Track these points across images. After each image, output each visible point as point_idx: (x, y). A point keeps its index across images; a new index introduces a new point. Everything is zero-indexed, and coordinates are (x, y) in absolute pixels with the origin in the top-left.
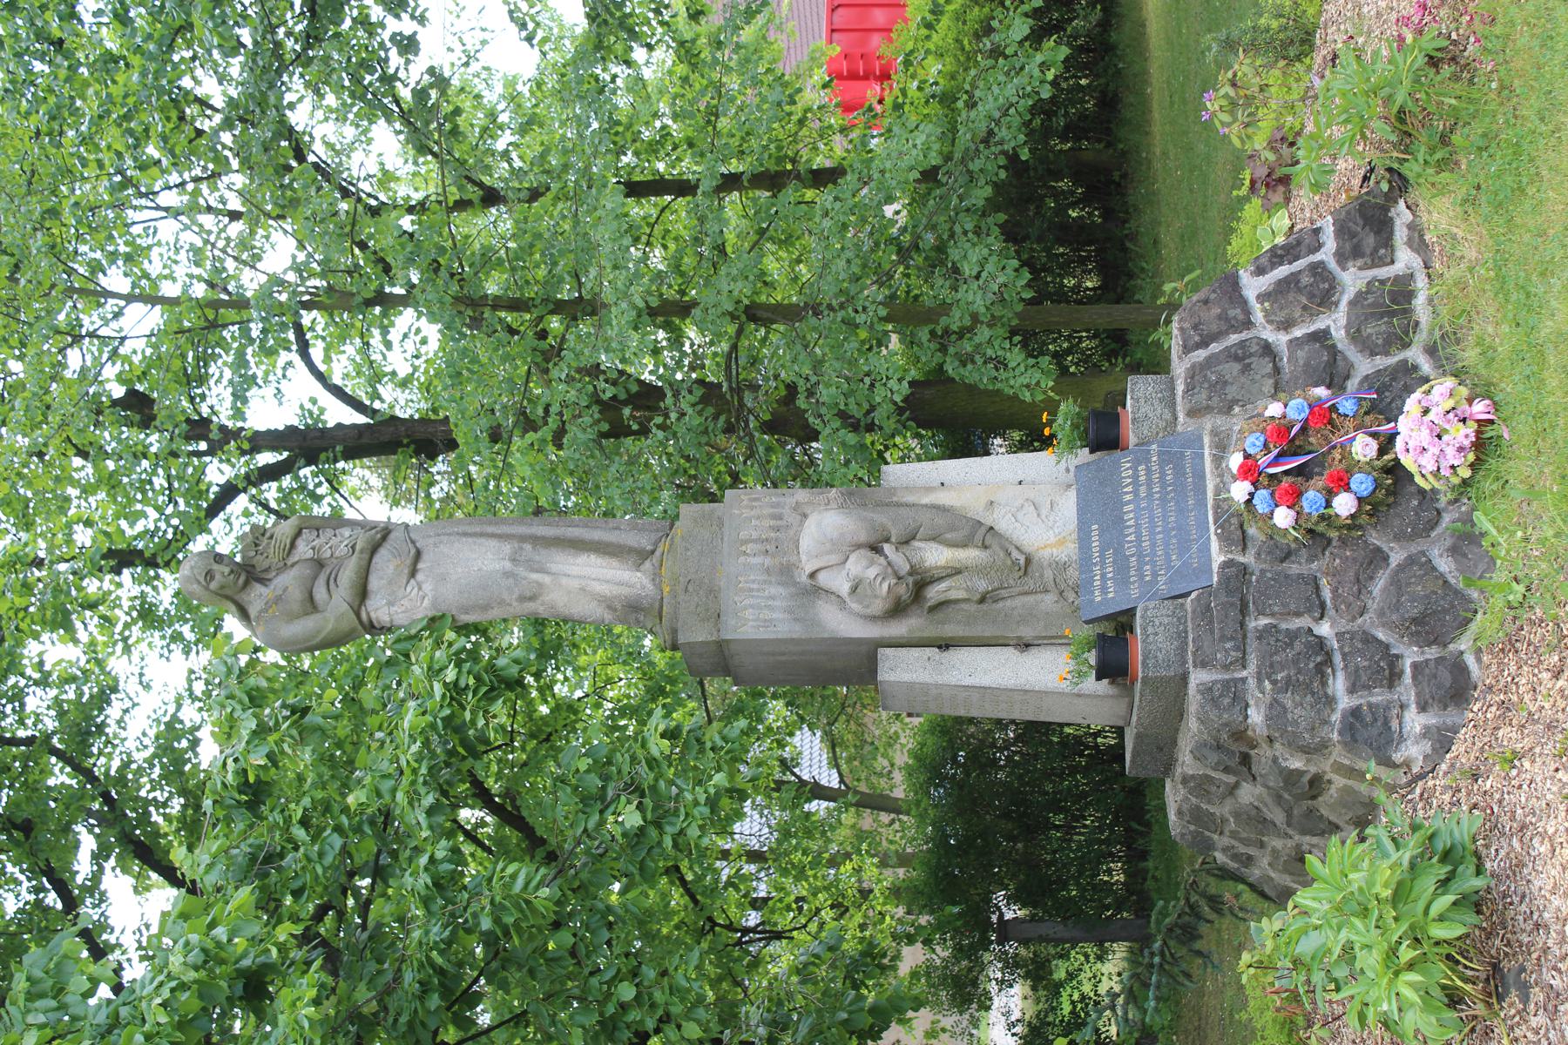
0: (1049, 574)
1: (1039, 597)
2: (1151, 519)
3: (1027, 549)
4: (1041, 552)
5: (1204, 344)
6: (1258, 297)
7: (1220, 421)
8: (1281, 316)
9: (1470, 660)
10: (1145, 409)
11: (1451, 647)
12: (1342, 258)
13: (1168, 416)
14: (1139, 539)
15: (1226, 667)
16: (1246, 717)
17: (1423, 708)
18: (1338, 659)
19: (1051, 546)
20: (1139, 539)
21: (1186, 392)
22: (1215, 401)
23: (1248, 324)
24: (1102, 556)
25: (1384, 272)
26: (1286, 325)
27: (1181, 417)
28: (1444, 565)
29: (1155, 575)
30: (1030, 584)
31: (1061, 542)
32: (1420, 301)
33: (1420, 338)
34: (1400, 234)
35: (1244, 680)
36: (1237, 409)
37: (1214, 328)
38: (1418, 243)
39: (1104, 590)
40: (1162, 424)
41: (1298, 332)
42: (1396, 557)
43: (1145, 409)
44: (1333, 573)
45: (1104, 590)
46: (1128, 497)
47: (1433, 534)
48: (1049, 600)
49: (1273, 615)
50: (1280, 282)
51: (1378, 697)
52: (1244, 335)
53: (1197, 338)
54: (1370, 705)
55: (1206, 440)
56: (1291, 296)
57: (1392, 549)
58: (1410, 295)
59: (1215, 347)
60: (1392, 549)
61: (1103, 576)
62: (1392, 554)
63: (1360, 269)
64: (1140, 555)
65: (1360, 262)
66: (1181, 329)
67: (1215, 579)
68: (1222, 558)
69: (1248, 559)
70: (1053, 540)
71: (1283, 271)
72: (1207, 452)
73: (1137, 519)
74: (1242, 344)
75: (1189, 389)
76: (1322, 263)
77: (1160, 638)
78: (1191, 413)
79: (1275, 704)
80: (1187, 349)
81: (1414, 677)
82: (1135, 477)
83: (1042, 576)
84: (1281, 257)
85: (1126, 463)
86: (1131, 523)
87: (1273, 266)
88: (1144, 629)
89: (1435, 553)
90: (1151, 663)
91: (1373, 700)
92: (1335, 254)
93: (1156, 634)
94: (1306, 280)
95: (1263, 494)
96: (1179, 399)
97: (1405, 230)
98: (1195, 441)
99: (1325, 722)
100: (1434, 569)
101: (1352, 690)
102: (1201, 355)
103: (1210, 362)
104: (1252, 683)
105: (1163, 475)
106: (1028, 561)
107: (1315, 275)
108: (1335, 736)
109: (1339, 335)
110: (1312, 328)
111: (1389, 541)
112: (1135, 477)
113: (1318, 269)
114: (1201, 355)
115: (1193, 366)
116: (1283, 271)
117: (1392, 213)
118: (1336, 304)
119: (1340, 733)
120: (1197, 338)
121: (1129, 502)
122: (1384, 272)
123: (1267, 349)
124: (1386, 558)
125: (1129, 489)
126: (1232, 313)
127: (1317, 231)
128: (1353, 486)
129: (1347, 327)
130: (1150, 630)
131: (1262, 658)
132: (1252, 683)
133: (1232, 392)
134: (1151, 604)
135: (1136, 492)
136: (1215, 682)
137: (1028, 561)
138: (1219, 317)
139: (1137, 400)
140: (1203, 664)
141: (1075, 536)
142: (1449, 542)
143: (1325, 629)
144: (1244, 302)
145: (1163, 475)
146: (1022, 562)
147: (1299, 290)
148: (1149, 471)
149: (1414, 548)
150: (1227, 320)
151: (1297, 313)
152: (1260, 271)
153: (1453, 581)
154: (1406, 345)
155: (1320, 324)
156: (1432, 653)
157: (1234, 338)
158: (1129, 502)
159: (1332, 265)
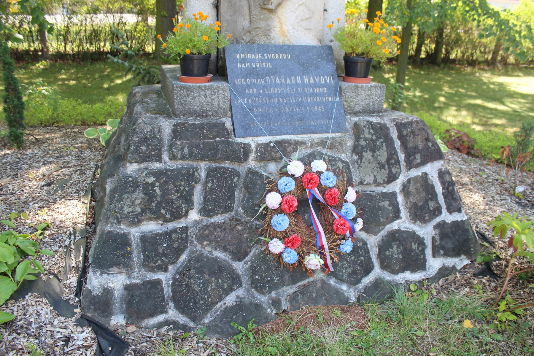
0: (262, 24)
1: (247, 17)
2: (288, 95)
3: (280, 11)
4: (277, 20)
5: (400, 137)
6: (426, 174)
7: (350, 143)
8: (412, 188)
9: (161, 318)
10: (363, 94)
11: (172, 304)
12: (441, 226)
13: (357, 108)
14: (276, 86)
15: (171, 146)
16: (131, 163)
17: (127, 288)
18: (171, 226)
19: (281, 27)
20: (276, 86)
21: (371, 123)
22: (363, 143)
23: (410, 166)
24: (269, 60)
25: (429, 252)
26: (405, 189)
27: (355, 119)
28: (230, 300)
29: (250, 96)
30: (256, 11)
31: (283, 34)
32: (408, 276)
33: (387, 276)
34: (450, 262)
35: (159, 159)
36: (355, 157)
37: (410, 145)
38: (444, 272)
39: (243, 61)
40: (353, 105)
41: (400, 199)
42: (240, 267)
43: (363, 94)
44: (235, 221)
45: (243, 61)
46: (306, 80)
47: (254, 290)
48: (246, 23)
49: (206, 182)
50: (433, 187)
51: (136, 257)
52: (403, 163)
53: (405, 133)
54: (130, 252)
55: (338, 135)
56: (423, 195)
57: (246, 263)
58: (413, 271)
59: (397, 144)
60: (246, 263)
61: (254, 61)
62: (242, 263)
63: (433, 238)
64: (264, 87)
65: (437, 238)
66: (411, 123)
67: (239, 140)
68: (253, 145)
69: (252, 163)
70: (285, 28)
71: (439, 189)
72: (330, 135)
73: (291, 85)
74: (398, 162)
75: (372, 125)
76: (440, 213)
77: (202, 98)
78: (356, 126)
79: (135, 185)
80: (400, 126)
81: (150, 282)
82: (320, 86)
83: (261, 19)
84: (448, 189)
85: (329, 80)
86: (288, 81)
87: (443, 183)
88: (210, 88)
89: (240, 292)
90: (184, 92)
91: (135, 255)
92: (444, 222)
93: (205, 96)
94: (432, 204)
95: (292, 185)
96: (367, 118)
97: (451, 266)
98: (339, 128)
99: (119, 222)
100: (227, 294)
101: (144, 239)
102: (394, 134)
103: (389, 141)
104: (156, 166)
105: (318, 104)
106: (271, 11)
107: (434, 210)
108: (108, 228)
109: (395, 225)
110: (401, 208)
111: (252, 262)
112: (320, 86)
113: (438, 211)
114: (394, 134)
115: (388, 129)
116: (439, 189)
117: (463, 257)
118: (415, 223)
119: (109, 232)
120: (405, 133)
121: (302, 80)
122: (429, 252)
123: (392, 178)
124: (239, 260)
125: (312, 81)
126: (418, 156)
127: (459, 211)
128: (289, 250)
129: (399, 231)
130: (208, 92)
131: (179, 170)
132: (156, 166)
133: (367, 155)
134: (227, 94)
135: (309, 85)
136: (160, 140)
137: (271, 11)
138: (416, 148)
139: (370, 90)
140: (175, 132)
141: (287, 43)
142: (247, 301)
143: (194, 216)
144: (423, 163)
145: (318, 104)
146: (270, 7)
147: (427, 201)
148: (322, 95)
149: (245, 280)
150: (414, 154)
151: (412, 199)
152: (442, 174)
153: (218, 306)
154: (384, 267)
155: (404, 213)
156: (167, 291)
157: (402, 156)
158: (302, 80)
159: (438, 220)
